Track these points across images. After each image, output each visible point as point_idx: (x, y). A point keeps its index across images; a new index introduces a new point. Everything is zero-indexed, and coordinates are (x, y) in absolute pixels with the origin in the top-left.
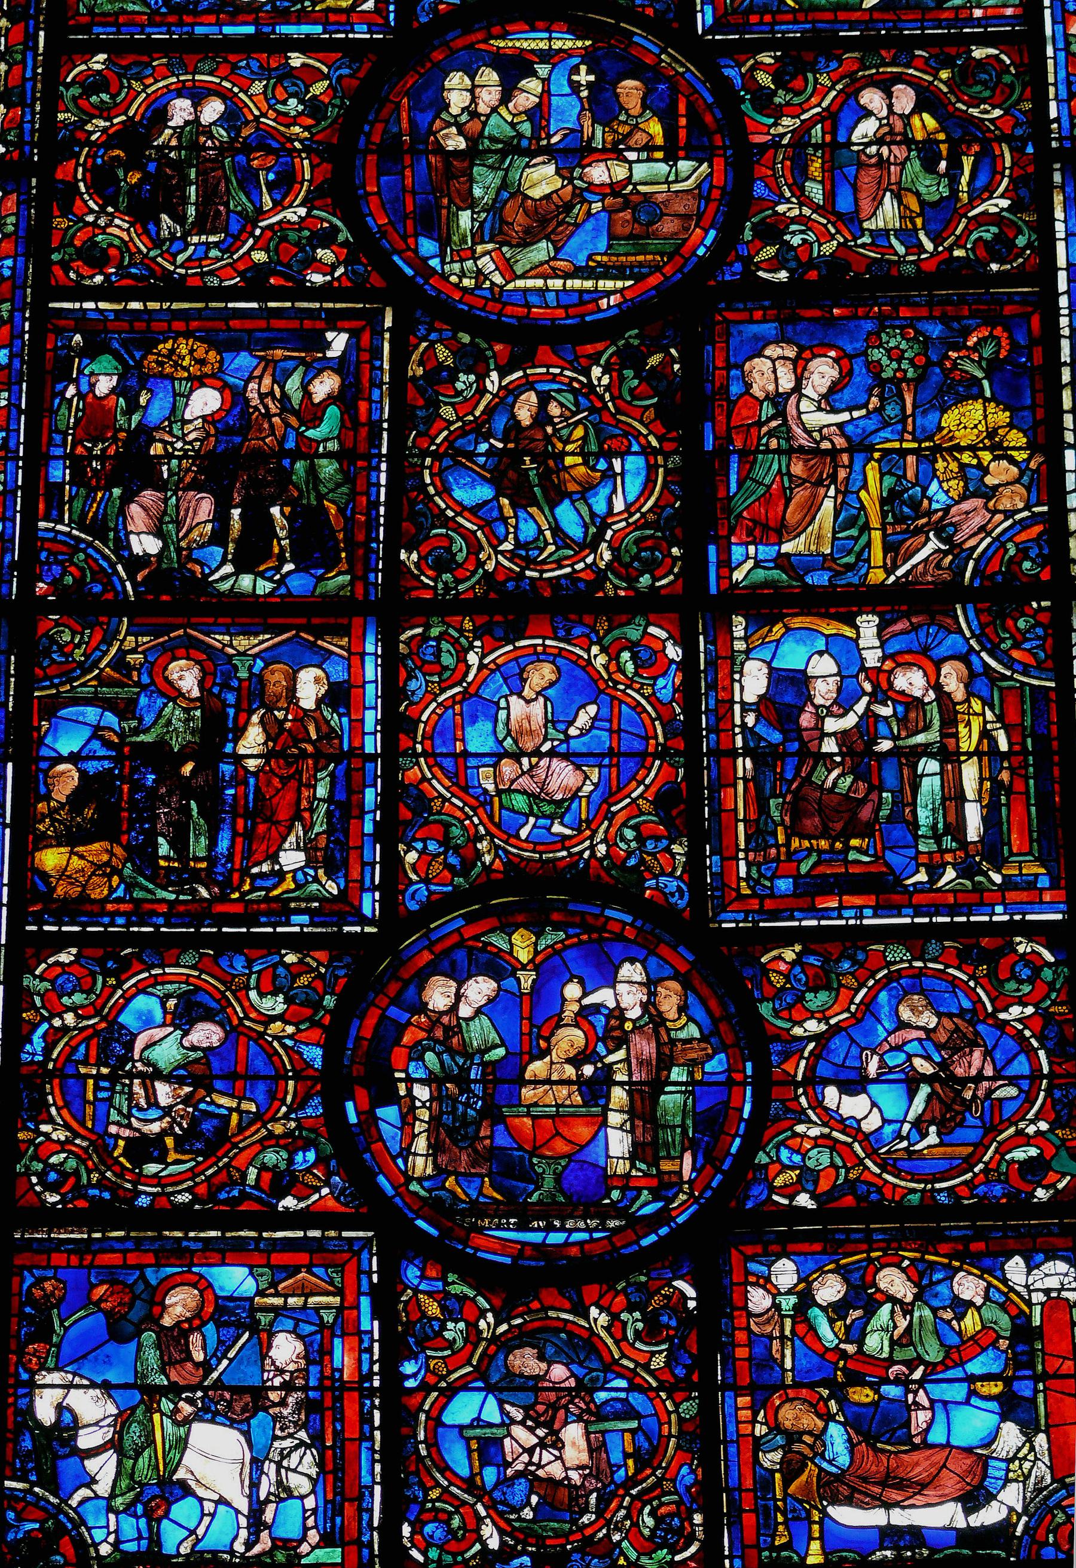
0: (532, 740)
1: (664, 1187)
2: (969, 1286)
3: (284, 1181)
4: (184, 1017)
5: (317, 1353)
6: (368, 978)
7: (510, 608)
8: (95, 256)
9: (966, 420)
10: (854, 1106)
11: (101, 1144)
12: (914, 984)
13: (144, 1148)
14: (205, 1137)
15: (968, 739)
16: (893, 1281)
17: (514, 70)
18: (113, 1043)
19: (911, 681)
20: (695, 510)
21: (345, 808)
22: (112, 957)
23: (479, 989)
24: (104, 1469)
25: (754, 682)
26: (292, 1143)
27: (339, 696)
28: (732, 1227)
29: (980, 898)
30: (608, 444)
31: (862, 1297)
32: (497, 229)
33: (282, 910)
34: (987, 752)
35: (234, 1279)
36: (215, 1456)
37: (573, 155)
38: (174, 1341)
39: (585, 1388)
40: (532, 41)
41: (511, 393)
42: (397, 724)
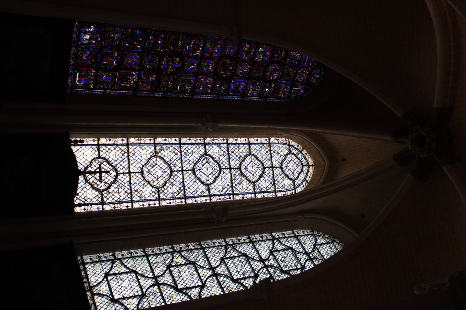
0: (133, 60)
1: (101, 65)
2: (92, 82)
3: (105, 43)
4: (117, 37)
5: (93, 43)
6: (118, 48)
7: (142, 59)
8: (171, 36)
9: (149, 87)
10: (105, 76)
11: (109, 32)
12: (112, 80)
13: (109, 34)
14: (109, 38)
15: (128, 85)
16: (93, 78)
17: (179, 63)
18: (117, 33)
19: (132, 82)
20: (146, 70)
21: (130, 48)
22: (122, 33)
23: (116, 55)
24: (88, 30)
25: (134, 73)
26: (108, 43)
27: (138, 48)
28: (97, 69)
29: (117, 84)
30: (152, 66)
31: (92, 76)
32: (168, 60)
33: (124, 44)
34: (127, 86)
35: (99, 39)
36: (88, 37)
37: (172, 66)
38: (95, 35)
39: (89, 59)
40: (180, 64)
41: (156, 60)
42: (135, 52)
